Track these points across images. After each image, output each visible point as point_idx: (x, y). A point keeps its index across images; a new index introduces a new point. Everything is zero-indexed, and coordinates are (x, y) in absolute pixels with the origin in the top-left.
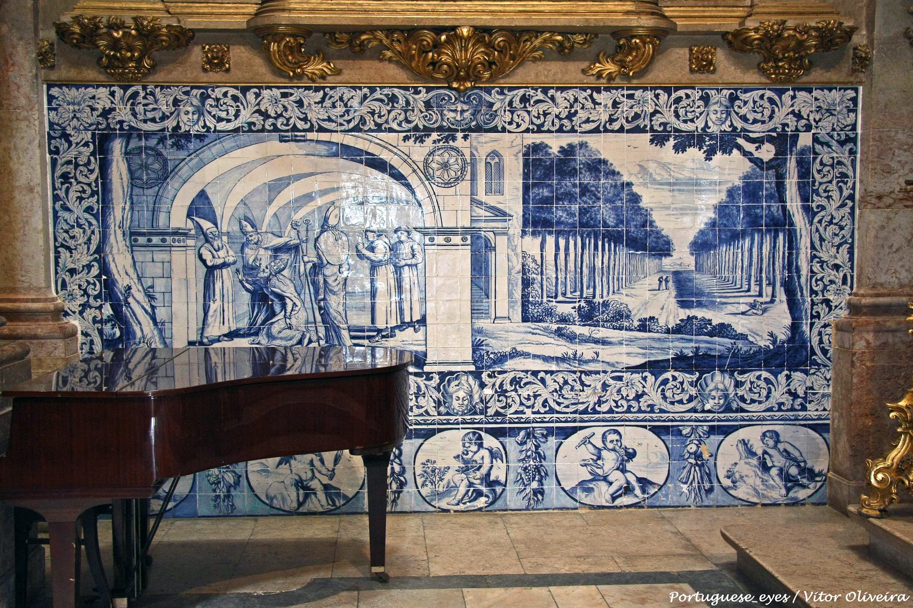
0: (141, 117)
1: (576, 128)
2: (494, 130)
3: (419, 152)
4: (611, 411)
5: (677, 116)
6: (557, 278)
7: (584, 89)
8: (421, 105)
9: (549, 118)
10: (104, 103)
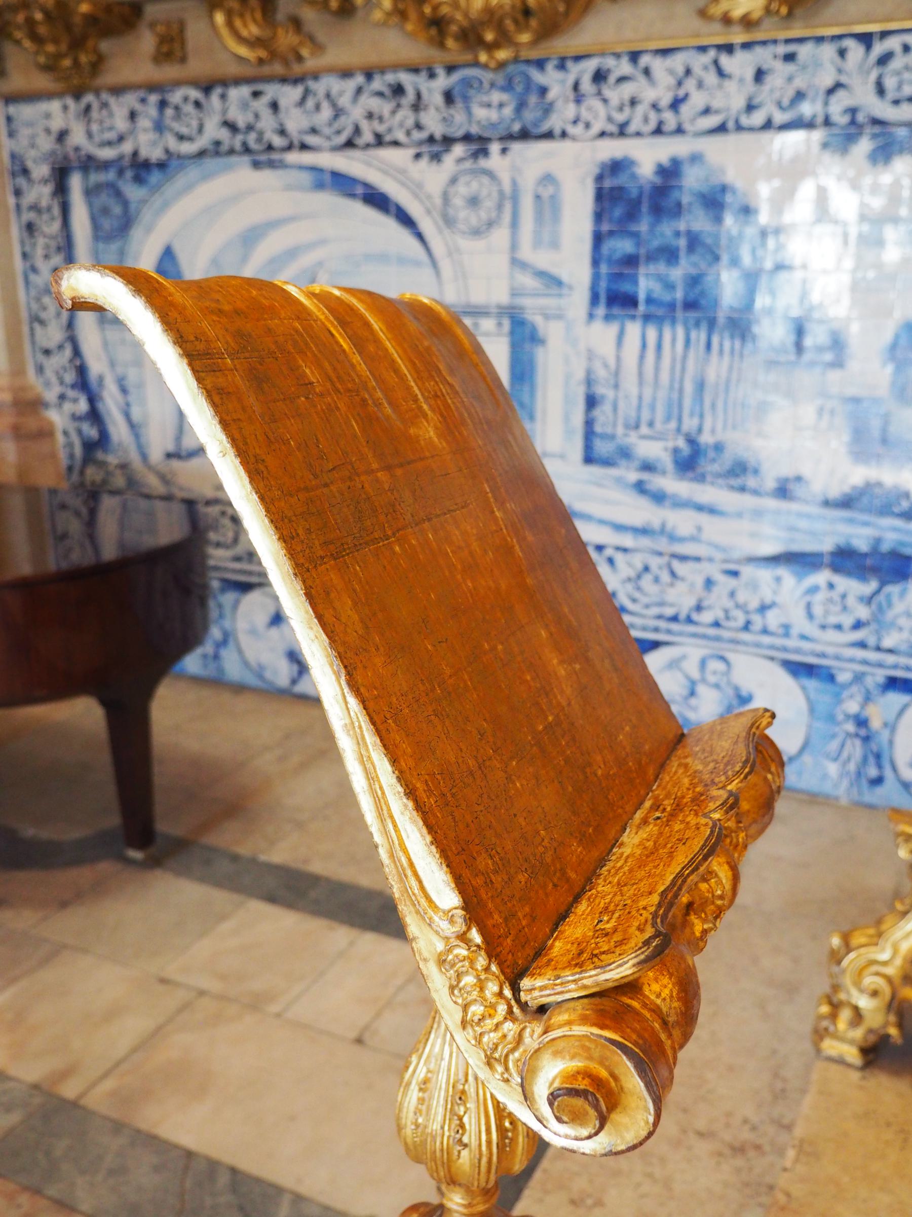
0: (97, 139)
1: (687, 126)
2: (549, 135)
3: (434, 176)
4: (717, 624)
5: (881, 90)
6: (640, 398)
7: (703, 49)
8: (439, 99)
9: (640, 110)
10: (57, 124)
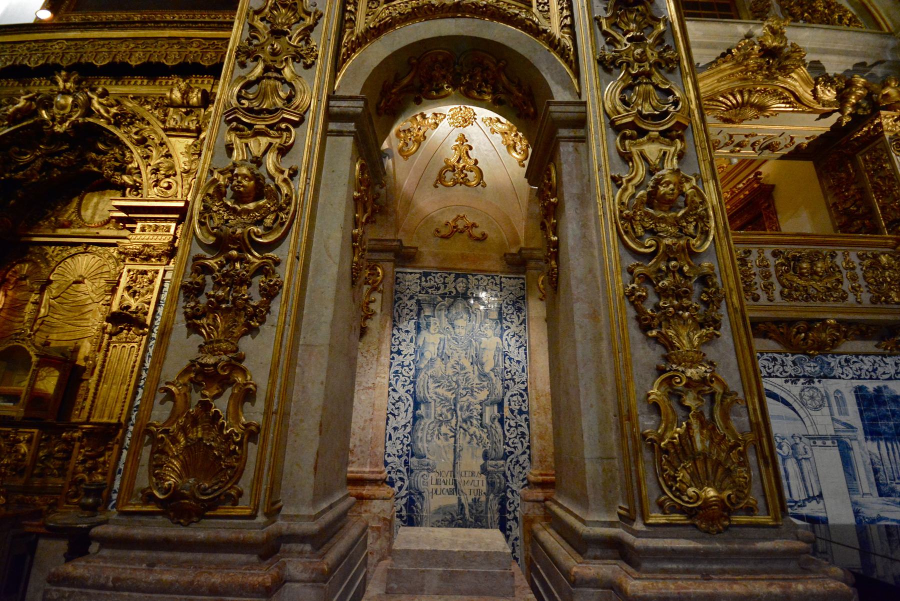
2: (834, 377)
3: (796, 389)
8: (791, 363)
